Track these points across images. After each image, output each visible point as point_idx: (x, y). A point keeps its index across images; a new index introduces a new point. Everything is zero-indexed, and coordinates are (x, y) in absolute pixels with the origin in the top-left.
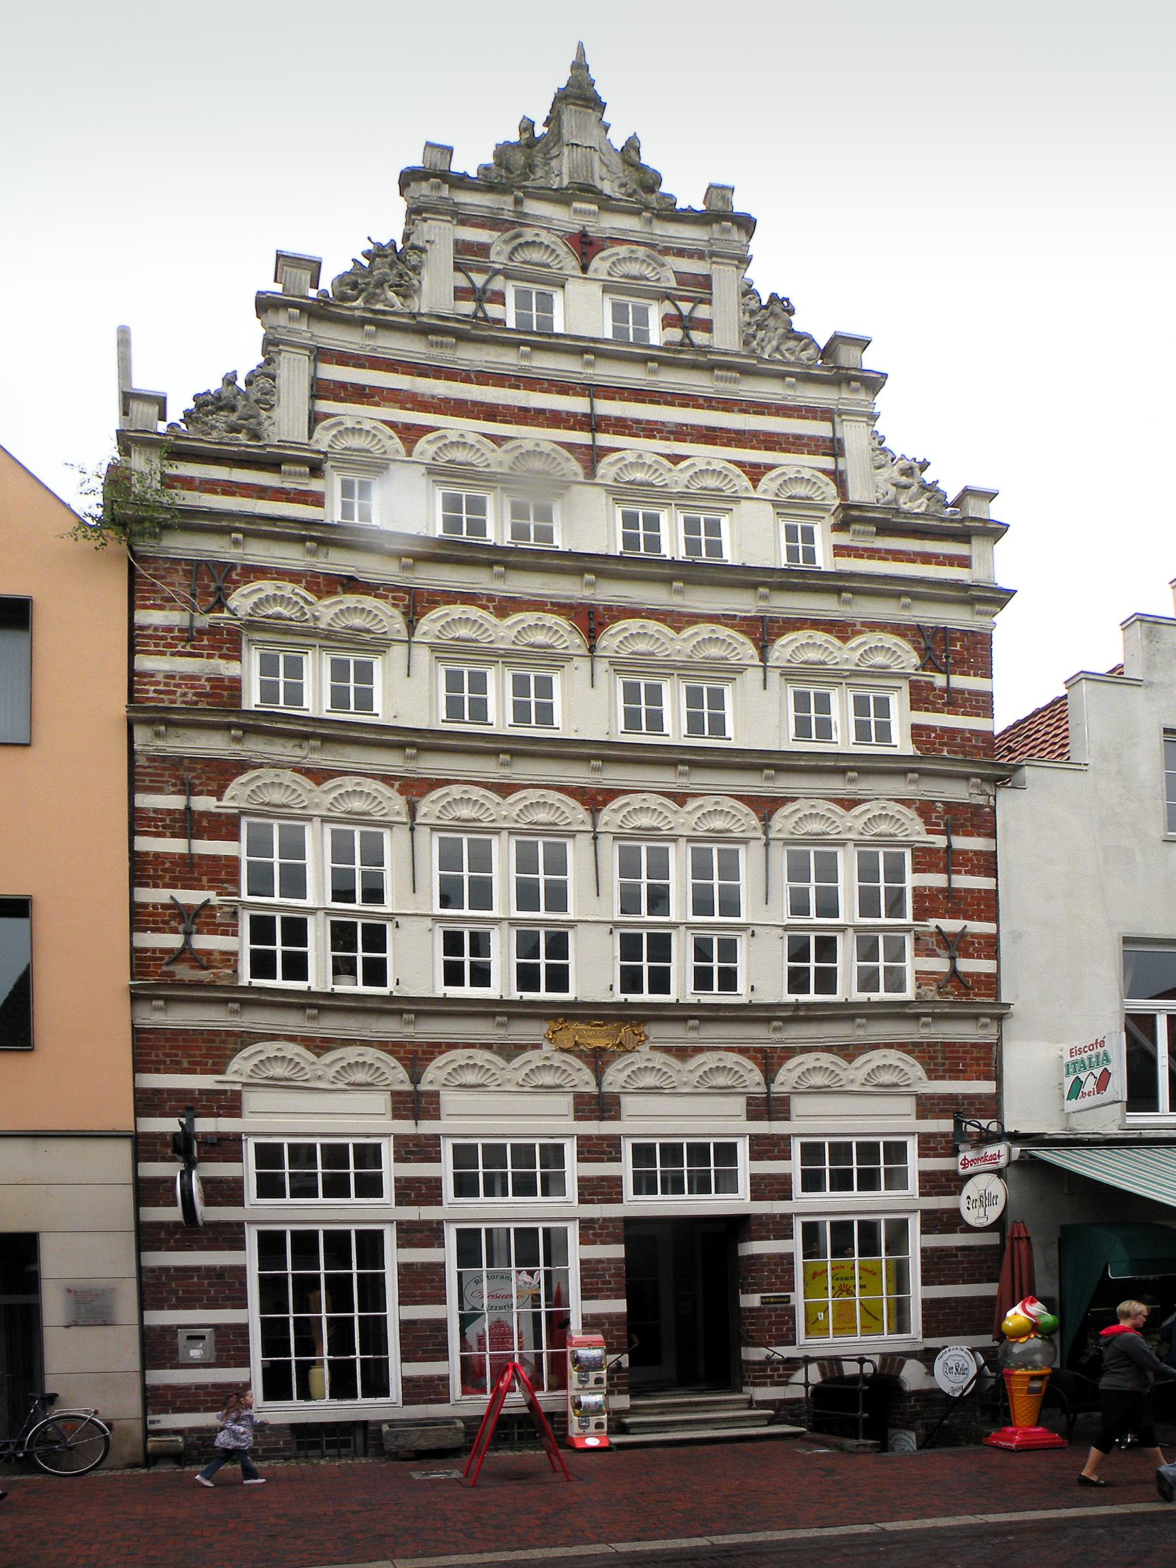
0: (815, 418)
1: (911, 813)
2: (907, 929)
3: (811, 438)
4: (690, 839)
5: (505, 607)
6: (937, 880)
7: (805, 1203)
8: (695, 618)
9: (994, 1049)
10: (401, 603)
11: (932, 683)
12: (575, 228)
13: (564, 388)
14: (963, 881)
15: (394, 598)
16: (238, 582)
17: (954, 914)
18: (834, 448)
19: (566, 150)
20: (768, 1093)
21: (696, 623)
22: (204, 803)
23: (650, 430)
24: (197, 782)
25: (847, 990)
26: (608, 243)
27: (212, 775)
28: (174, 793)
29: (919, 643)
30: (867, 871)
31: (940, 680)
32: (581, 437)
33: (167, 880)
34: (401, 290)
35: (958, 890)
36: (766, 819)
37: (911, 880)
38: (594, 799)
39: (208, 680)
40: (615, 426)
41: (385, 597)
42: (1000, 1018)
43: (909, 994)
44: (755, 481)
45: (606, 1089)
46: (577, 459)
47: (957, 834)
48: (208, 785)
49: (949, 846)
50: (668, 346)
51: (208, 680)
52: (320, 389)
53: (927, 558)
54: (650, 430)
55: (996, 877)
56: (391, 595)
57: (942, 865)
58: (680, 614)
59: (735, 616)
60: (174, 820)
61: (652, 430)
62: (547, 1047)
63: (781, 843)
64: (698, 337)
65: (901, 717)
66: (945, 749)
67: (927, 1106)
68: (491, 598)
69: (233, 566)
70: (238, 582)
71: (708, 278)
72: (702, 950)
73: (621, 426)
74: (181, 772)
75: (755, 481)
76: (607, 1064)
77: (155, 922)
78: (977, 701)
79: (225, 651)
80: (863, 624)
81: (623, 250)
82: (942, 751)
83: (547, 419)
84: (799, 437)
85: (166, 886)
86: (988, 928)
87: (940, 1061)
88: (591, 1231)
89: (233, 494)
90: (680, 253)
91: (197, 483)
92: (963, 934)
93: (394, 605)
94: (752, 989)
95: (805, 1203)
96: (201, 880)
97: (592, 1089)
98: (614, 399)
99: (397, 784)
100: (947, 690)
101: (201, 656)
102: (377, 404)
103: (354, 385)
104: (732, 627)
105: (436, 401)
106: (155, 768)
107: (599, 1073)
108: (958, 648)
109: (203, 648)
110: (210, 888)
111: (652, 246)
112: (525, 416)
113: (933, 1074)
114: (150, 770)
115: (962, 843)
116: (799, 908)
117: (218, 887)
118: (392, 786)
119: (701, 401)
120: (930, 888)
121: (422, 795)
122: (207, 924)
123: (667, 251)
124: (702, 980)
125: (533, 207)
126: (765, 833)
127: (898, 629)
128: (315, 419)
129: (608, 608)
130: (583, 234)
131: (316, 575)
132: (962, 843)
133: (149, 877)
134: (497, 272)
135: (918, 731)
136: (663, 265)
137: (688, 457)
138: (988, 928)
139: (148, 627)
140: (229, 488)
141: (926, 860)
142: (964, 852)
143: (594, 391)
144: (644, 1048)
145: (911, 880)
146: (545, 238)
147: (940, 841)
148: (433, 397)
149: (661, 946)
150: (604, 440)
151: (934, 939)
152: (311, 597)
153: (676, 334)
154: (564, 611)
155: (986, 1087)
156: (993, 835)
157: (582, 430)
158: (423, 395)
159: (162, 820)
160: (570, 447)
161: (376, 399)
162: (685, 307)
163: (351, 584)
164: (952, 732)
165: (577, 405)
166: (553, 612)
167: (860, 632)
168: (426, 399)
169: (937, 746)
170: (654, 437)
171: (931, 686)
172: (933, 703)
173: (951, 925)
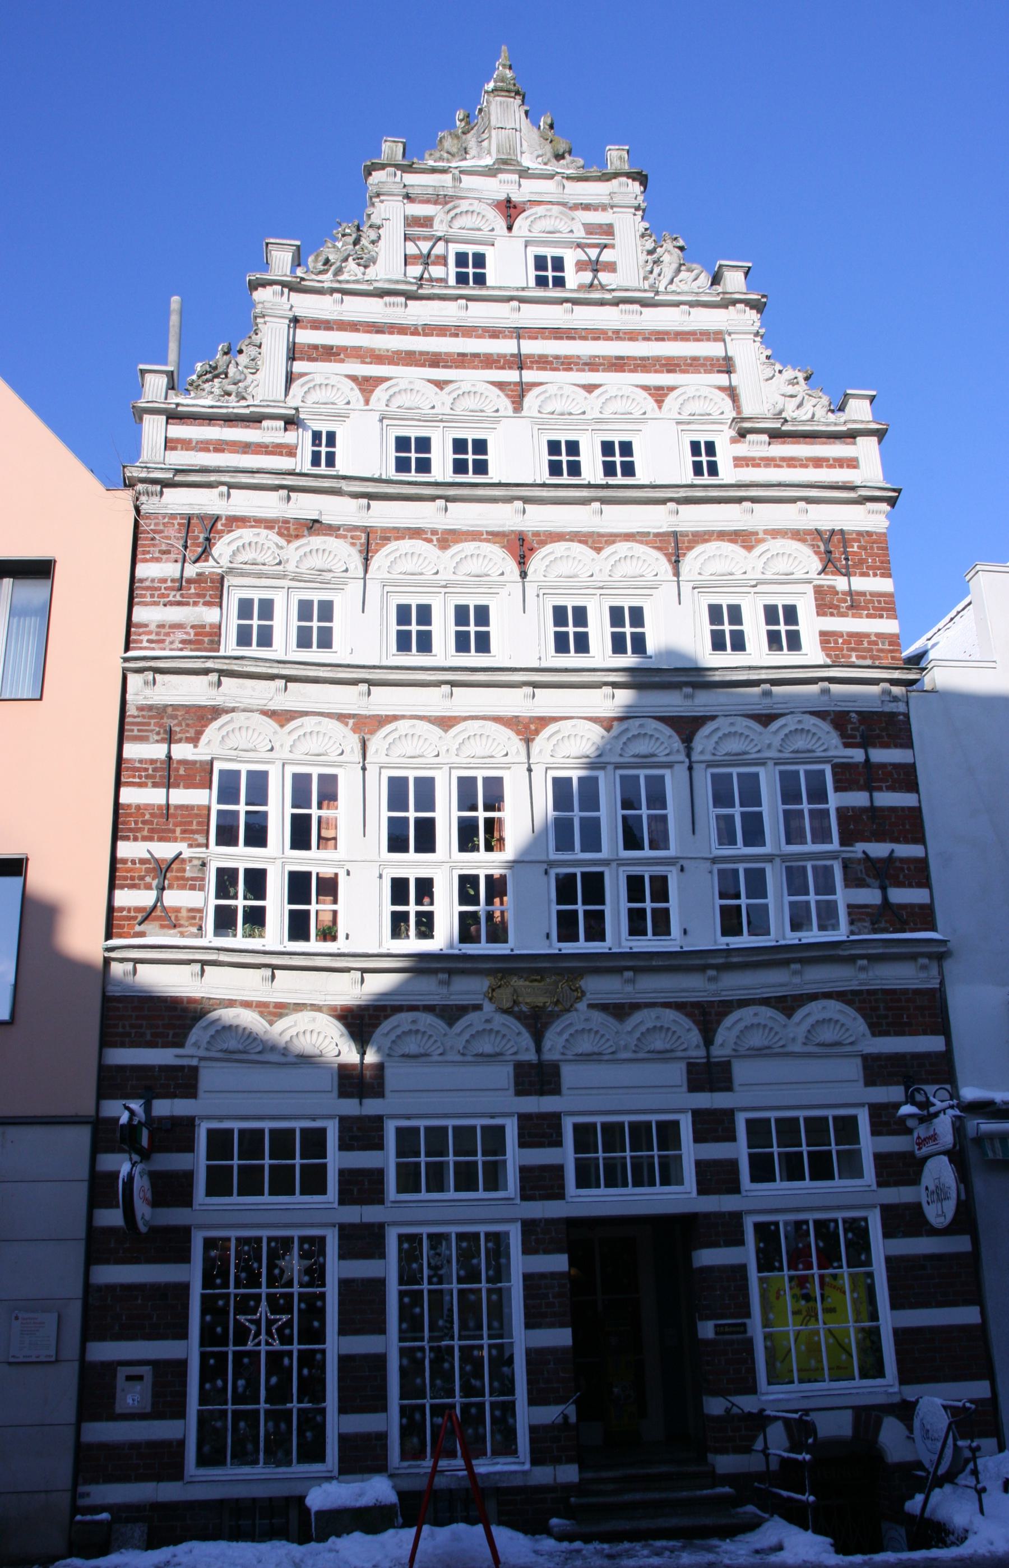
0: (708, 340)
1: (826, 726)
2: (833, 856)
3: (706, 358)
4: (618, 766)
5: (447, 539)
6: (858, 799)
7: (760, 1199)
8: (612, 538)
9: (938, 995)
10: (358, 542)
11: (834, 587)
12: (502, 197)
13: (495, 333)
14: (886, 799)
15: (352, 538)
16: (222, 531)
17: (879, 837)
18: (727, 366)
19: (494, 132)
20: (708, 1056)
21: (614, 542)
22: (182, 751)
23: (567, 363)
24: (177, 729)
25: (780, 933)
26: (528, 205)
27: (190, 722)
28: (157, 741)
29: (818, 547)
30: (790, 794)
31: (841, 583)
32: (511, 376)
33: (145, 833)
34: (362, 262)
35: (882, 809)
36: (688, 741)
37: (834, 800)
38: (526, 727)
39: (192, 627)
40: (537, 362)
41: (345, 537)
42: (940, 957)
43: (841, 933)
44: (660, 402)
45: (548, 1056)
46: (507, 396)
47: (874, 746)
48: (188, 732)
49: (867, 759)
50: (581, 287)
51: (192, 627)
52: (294, 353)
53: (818, 462)
54: (567, 363)
55: (917, 792)
56: (349, 534)
57: (862, 782)
58: (600, 535)
59: (649, 533)
60: (155, 770)
61: (570, 364)
62: (488, 1007)
63: (703, 766)
64: (604, 277)
65: (810, 625)
66: (854, 654)
67: (877, 1069)
68: (434, 532)
69: (218, 518)
70: (222, 531)
71: (610, 226)
72: (635, 886)
73: (543, 362)
74: (165, 720)
75: (660, 402)
76: (546, 1026)
77: (132, 878)
78: (879, 602)
79: (208, 598)
80: (766, 532)
81: (540, 210)
82: (850, 656)
83: (481, 362)
84: (695, 359)
85: (145, 839)
86: (913, 851)
87: (882, 1012)
88: (537, 1236)
89: (222, 451)
90: (587, 207)
91: (194, 444)
92: (891, 859)
93: (353, 544)
94: (685, 932)
95: (760, 1199)
96: (174, 831)
97: (531, 1056)
98: (536, 338)
99: (351, 722)
100: (850, 593)
101: (187, 604)
102: (342, 361)
103: (324, 347)
104: (647, 543)
105: (390, 354)
106: (144, 717)
107: (538, 1038)
108: (855, 549)
109: (189, 596)
110: (183, 840)
111: (564, 204)
112: (463, 360)
113: (877, 1029)
114: (138, 720)
115: (880, 755)
116: (727, 836)
117: (189, 839)
118: (347, 724)
119: (610, 334)
120: (853, 808)
121: (372, 732)
122: (178, 878)
123: (576, 207)
124: (636, 924)
125: (467, 181)
126: (689, 756)
127: (797, 535)
128: (290, 378)
129: (537, 534)
130: (509, 201)
131: (286, 521)
132: (880, 755)
133: (131, 830)
134: (440, 239)
135: (826, 637)
136: (573, 219)
137: (600, 386)
138: (913, 851)
139: (146, 579)
140: (220, 447)
141: (848, 777)
142: (883, 766)
143: (519, 333)
144: (582, 1006)
145: (834, 800)
146: (476, 206)
147: (857, 755)
148: (388, 351)
149: (595, 887)
150: (529, 376)
151: (862, 867)
152: (282, 542)
153: (587, 277)
154: (497, 539)
155: (934, 1043)
156: (909, 744)
157: (510, 368)
158: (379, 350)
159: (146, 770)
160: (500, 385)
161: (342, 356)
162: (593, 253)
163: (314, 526)
164: (858, 637)
165: (507, 347)
166: (487, 541)
167: (763, 540)
168: (382, 353)
169: (845, 652)
170: (571, 369)
171: (833, 591)
172: (837, 607)
173: (879, 850)
